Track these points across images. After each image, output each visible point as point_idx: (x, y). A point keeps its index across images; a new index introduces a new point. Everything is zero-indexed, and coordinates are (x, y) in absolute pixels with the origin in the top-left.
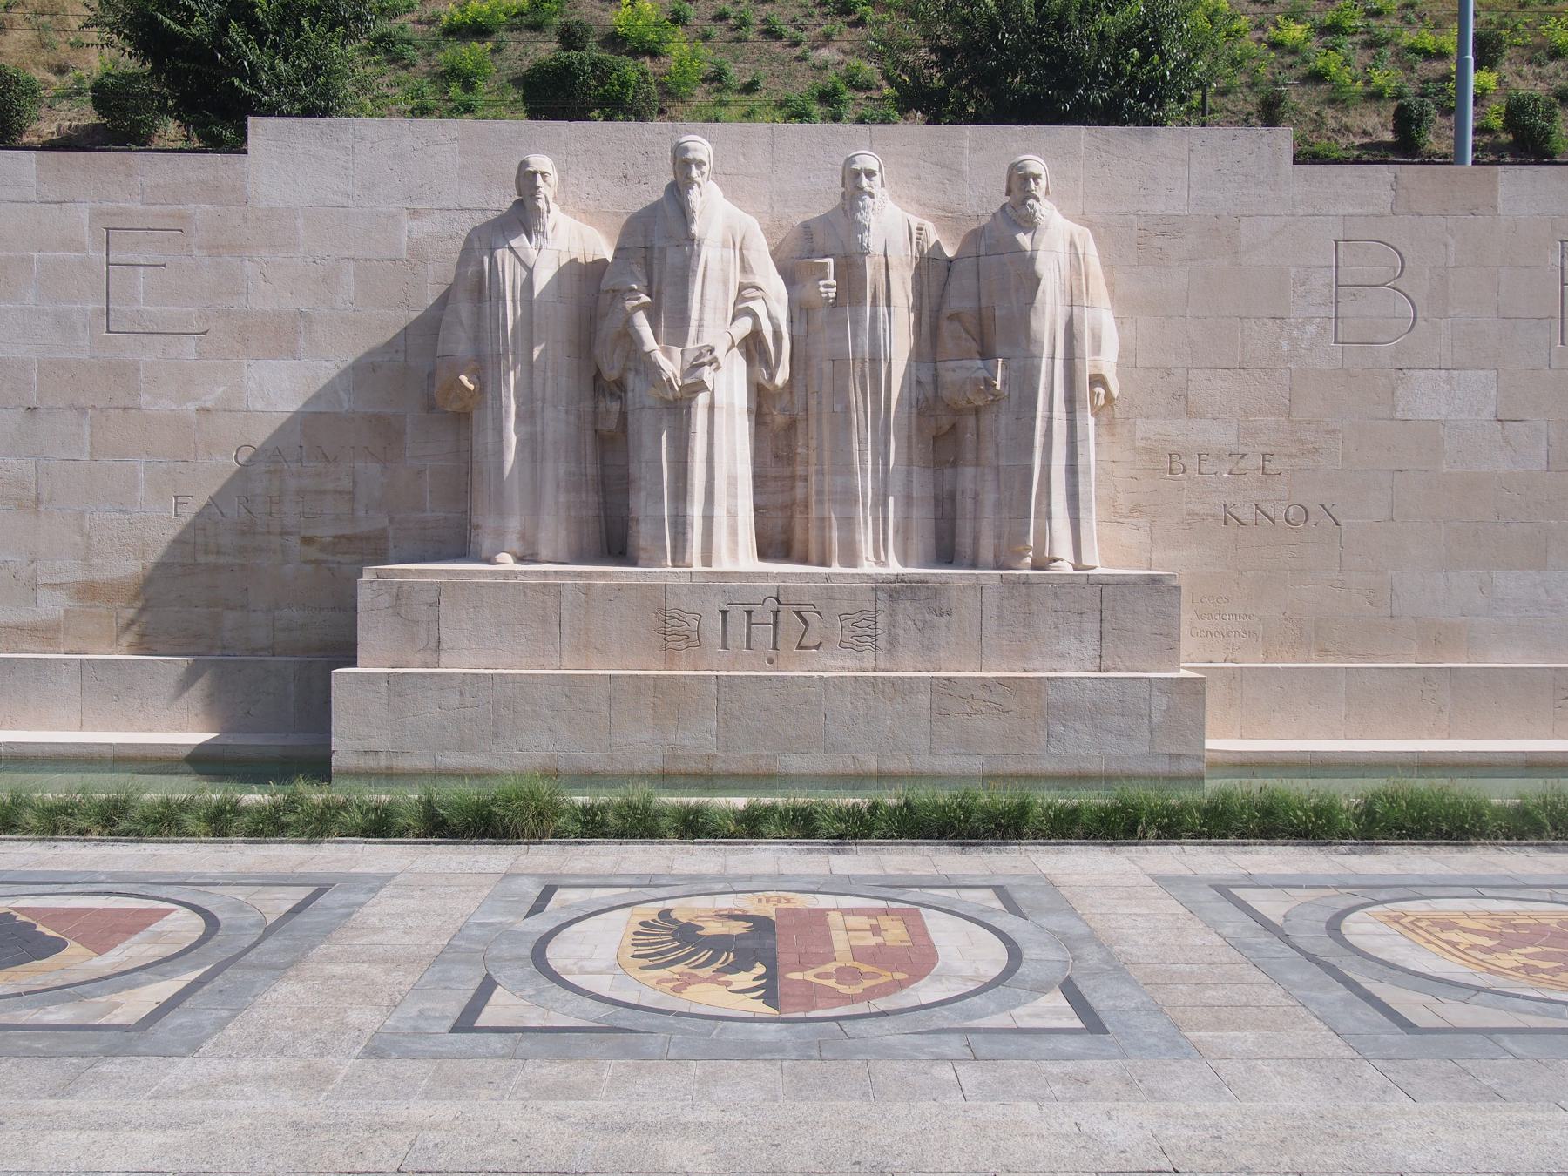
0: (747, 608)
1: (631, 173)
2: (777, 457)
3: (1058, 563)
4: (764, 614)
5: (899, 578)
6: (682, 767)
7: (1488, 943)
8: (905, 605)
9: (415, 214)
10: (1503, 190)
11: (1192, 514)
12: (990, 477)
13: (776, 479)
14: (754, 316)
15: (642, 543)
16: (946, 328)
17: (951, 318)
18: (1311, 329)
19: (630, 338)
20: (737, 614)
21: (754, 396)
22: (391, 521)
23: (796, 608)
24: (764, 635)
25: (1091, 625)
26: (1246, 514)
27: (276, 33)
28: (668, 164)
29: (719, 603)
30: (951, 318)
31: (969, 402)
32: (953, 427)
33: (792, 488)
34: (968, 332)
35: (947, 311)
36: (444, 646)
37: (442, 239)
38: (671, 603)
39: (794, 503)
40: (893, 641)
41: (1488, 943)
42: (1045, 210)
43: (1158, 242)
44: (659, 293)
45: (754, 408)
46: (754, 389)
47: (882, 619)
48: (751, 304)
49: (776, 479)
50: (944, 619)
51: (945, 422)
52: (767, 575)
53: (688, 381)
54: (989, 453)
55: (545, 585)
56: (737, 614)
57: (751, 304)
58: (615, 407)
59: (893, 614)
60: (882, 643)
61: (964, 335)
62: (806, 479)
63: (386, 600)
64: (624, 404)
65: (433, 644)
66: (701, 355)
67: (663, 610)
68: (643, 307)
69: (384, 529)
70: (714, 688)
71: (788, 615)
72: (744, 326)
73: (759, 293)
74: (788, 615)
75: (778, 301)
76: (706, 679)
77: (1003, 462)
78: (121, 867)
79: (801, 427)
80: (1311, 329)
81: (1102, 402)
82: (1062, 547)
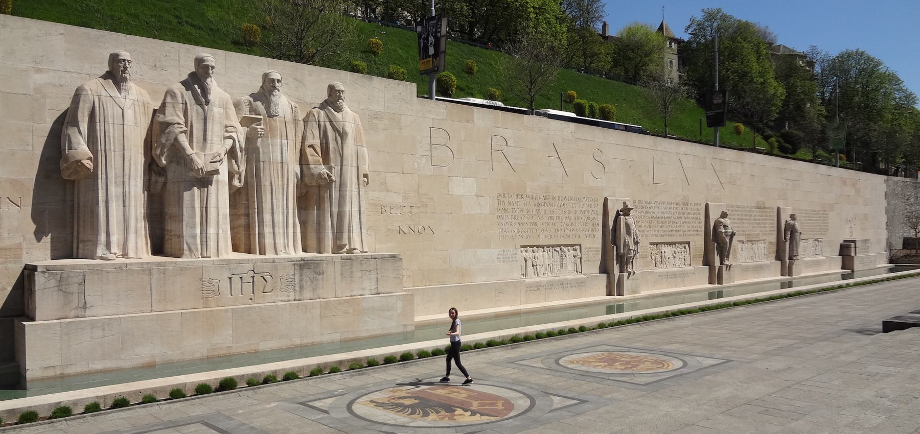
1: (158, 64)
4: (247, 278)
5: (303, 259)
6: (216, 353)
7: (787, 342)
8: (307, 272)
9: (39, 71)
10: (476, 115)
11: (388, 230)
14: (234, 140)
15: (185, 247)
16: (309, 151)
17: (310, 146)
18: (424, 160)
20: (236, 279)
22: (24, 239)
24: (248, 288)
25: (373, 276)
26: (406, 230)
27: (728, 70)
29: (227, 275)
30: (310, 146)
32: (307, 193)
35: (308, 143)
36: (88, 305)
37: (54, 86)
38: (205, 276)
40: (301, 287)
41: (787, 342)
42: (345, 105)
43: (375, 121)
44: (192, 126)
47: (297, 278)
50: (321, 276)
51: (304, 191)
53: (210, 169)
55: (143, 270)
56: (236, 279)
59: (301, 275)
60: (297, 288)
63: (53, 283)
64: (166, 179)
65: (81, 305)
66: (215, 157)
67: (202, 280)
68: (185, 132)
69: (20, 244)
70: (230, 314)
71: (258, 278)
72: (229, 143)
73: (234, 130)
74: (258, 278)
76: (226, 311)
78: (491, 392)
80: (424, 160)
82: (356, 244)
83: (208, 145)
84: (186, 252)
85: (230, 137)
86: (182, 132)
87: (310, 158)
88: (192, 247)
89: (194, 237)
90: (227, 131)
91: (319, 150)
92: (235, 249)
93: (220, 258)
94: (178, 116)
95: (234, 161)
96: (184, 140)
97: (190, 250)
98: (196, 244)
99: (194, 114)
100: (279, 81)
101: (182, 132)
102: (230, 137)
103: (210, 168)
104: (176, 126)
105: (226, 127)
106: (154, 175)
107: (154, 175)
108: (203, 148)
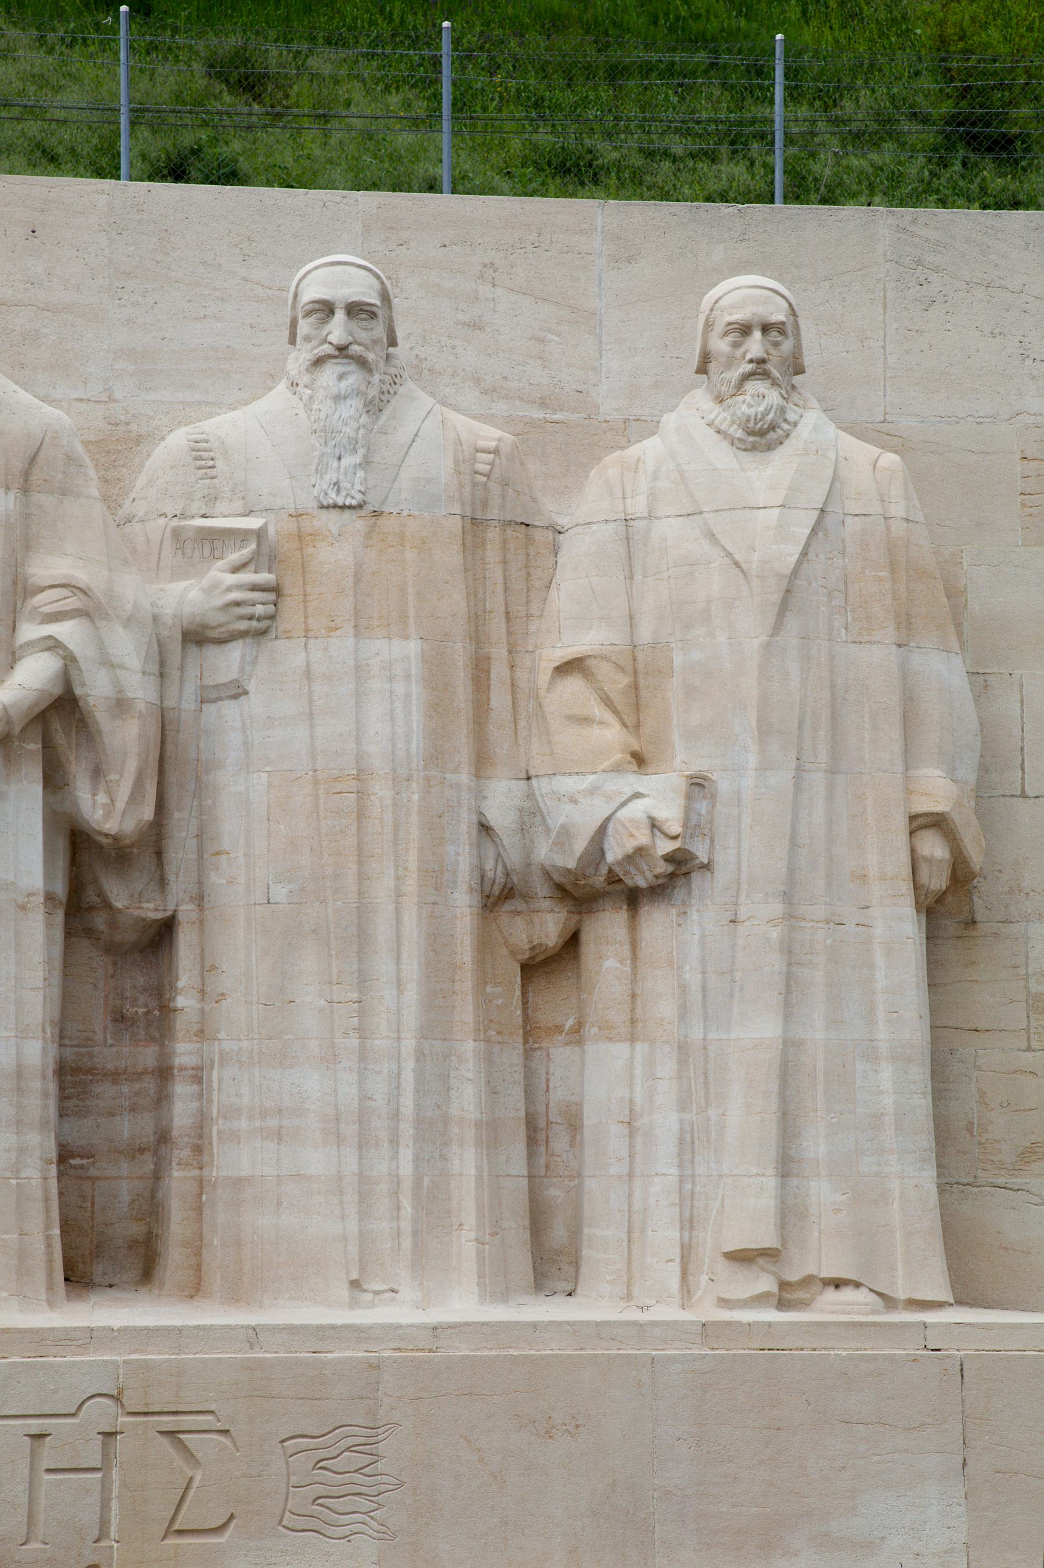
0: (35, 1425)
2: (119, 1018)
3: (847, 1294)
12: (667, 1066)
13: (116, 1076)
14: (70, 660)
21: (61, 863)
23: (168, 1422)
31: (613, 879)
33: (162, 1099)
34: (608, 703)
39: (163, 1137)
45: (60, 889)
46: (62, 844)
49: (116, 1076)
51: (549, 926)
52: (90, 1337)
54: (665, 1009)
57: (63, 630)
61: (599, 711)
62: (198, 1076)
75: (128, 622)
77: (696, 1034)
79: (185, 939)
81: (938, 881)
85: (52, 645)
87: (567, 737)
91: (617, 683)
92: (78, 1275)
100: (354, 310)
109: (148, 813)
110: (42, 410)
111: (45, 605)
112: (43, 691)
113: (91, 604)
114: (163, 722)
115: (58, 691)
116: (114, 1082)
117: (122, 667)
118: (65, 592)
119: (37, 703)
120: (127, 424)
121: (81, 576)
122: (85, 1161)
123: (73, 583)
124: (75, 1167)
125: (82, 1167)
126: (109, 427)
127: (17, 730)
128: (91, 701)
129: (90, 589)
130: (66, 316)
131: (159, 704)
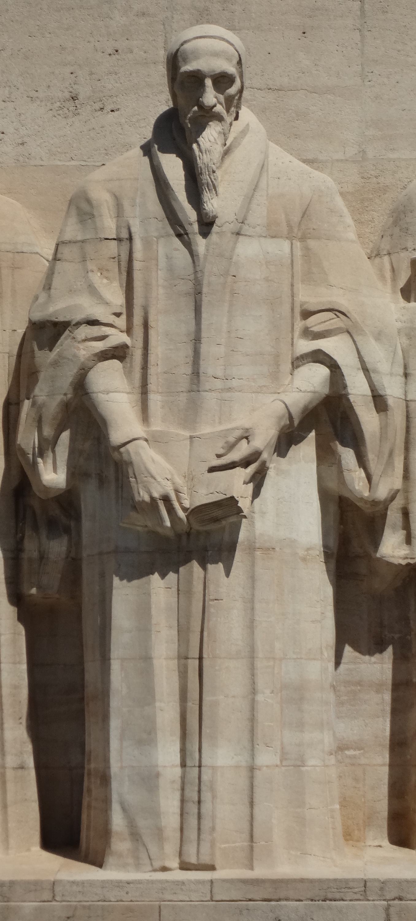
1: (84, 92)
14: (334, 367)
15: (118, 821)
19: (83, 416)
28: (160, 74)
46: (333, 508)
48: (324, 344)
58: (57, 548)
64: (76, 544)
66: (231, 447)
68: (119, 353)
75: (379, 336)
83: (210, 400)
84: (120, 845)
86: (104, 356)
88: (142, 823)
89: (149, 780)
90: (308, 334)
93: (260, 872)
94: (92, 291)
95: (348, 456)
96: (113, 392)
97: (135, 835)
98: (155, 813)
99: (160, 277)
101: (104, 356)
102: (319, 357)
103: (207, 491)
104: (85, 331)
105: (307, 314)
106: (28, 532)
107: (28, 532)
108: (190, 413)
109: (398, 483)
110: (311, 175)
111: (315, 325)
112: (314, 392)
113: (350, 323)
114: (407, 412)
115: (326, 391)
116: (378, 692)
117: (375, 371)
118: (330, 315)
119: (310, 402)
120: (376, 177)
121: (342, 301)
122: (357, 752)
123: (336, 308)
124: (350, 757)
125: (354, 757)
126: (363, 180)
127: (296, 422)
128: (352, 398)
129: (349, 312)
130: (329, 96)
131: (404, 397)
